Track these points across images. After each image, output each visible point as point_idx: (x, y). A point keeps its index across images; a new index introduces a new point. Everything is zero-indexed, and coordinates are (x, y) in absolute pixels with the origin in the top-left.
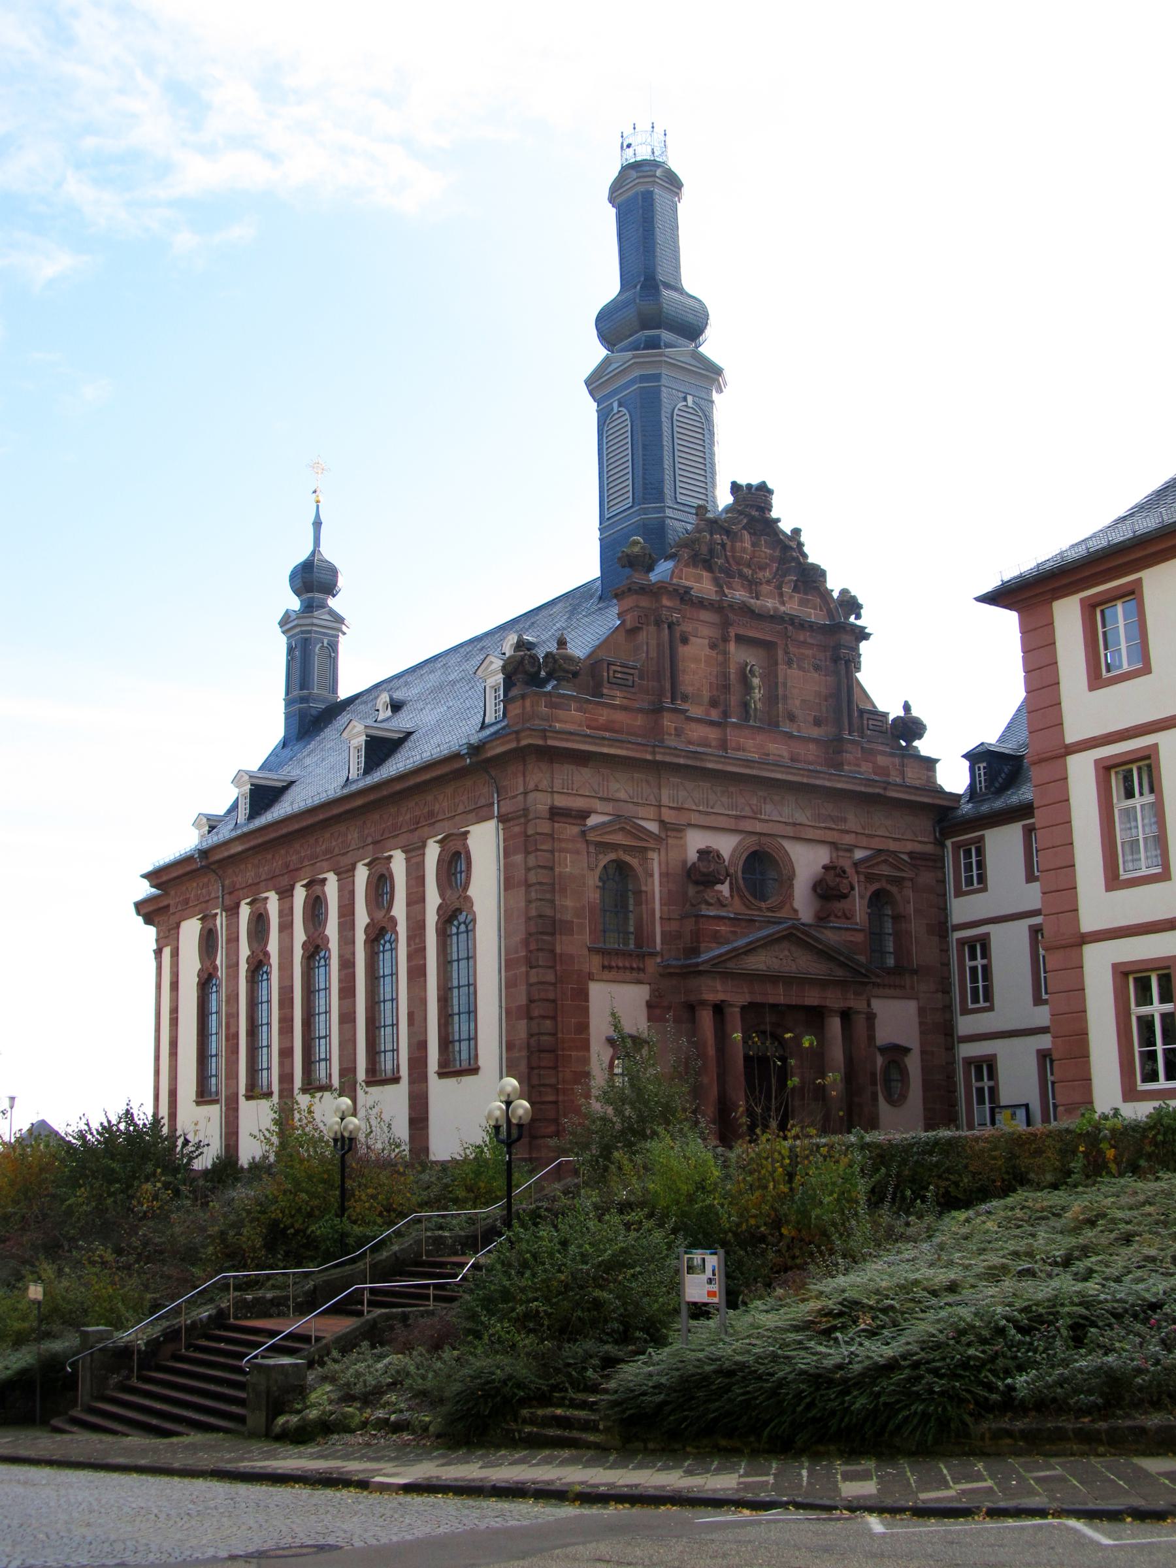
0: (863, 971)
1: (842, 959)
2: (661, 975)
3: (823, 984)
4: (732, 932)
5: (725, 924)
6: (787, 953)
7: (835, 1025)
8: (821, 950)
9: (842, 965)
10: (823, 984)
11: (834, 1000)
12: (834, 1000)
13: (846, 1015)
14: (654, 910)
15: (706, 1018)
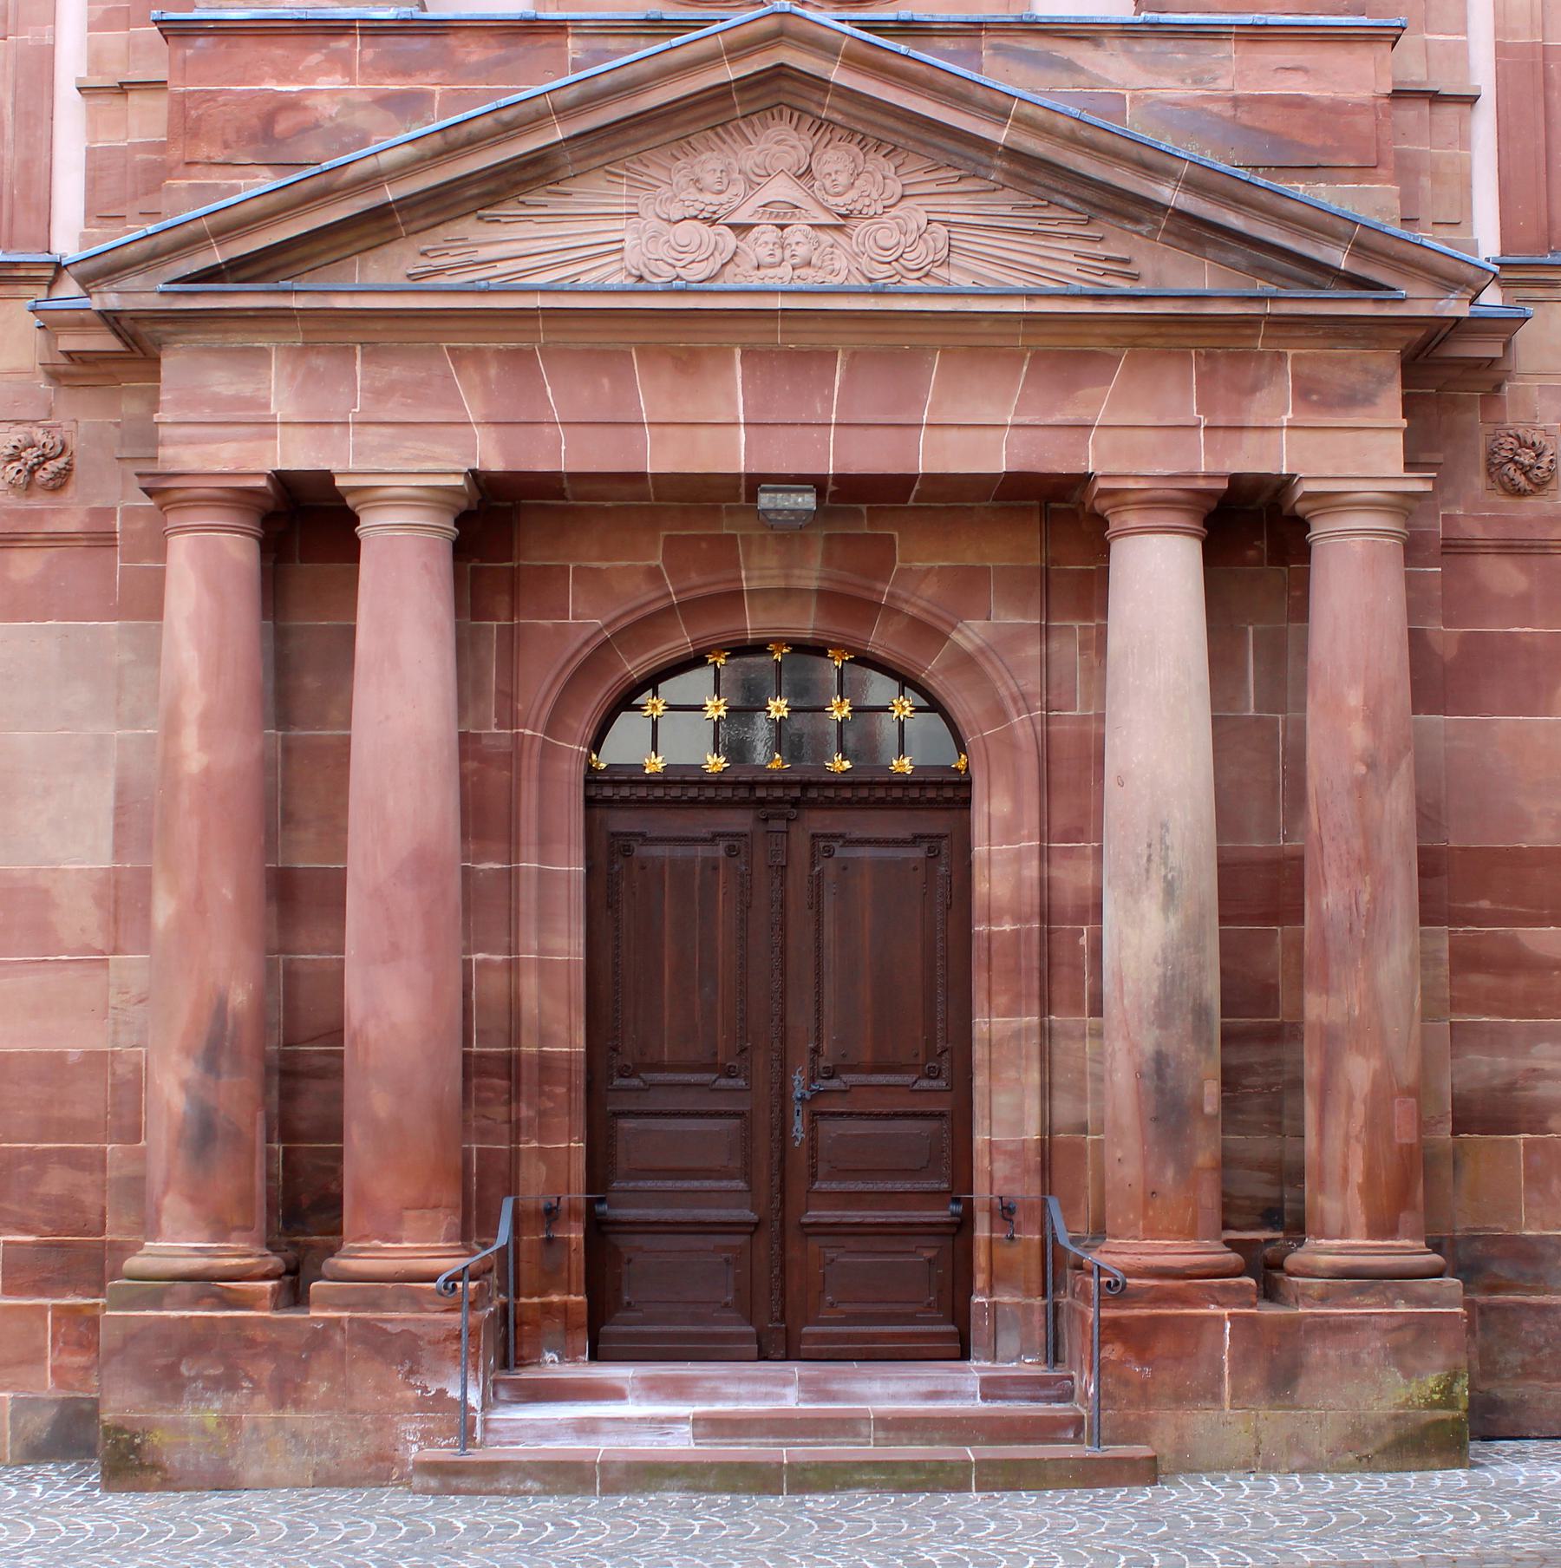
0: (1340, 258)
1: (1167, 193)
2: (55, 376)
3: (1063, 345)
4: (386, 101)
5: (344, 64)
6: (781, 189)
7: (1158, 580)
8: (1012, 154)
9: (1193, 232)
10: (1063, 345)
11: (1137, 434)
12: (1137, 434)
13: (1254, 534)
14: (45, 57)
15: (204, 575)
